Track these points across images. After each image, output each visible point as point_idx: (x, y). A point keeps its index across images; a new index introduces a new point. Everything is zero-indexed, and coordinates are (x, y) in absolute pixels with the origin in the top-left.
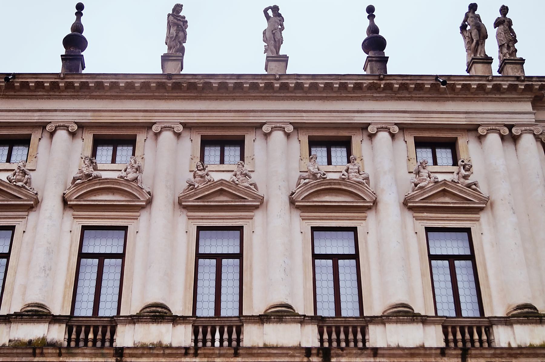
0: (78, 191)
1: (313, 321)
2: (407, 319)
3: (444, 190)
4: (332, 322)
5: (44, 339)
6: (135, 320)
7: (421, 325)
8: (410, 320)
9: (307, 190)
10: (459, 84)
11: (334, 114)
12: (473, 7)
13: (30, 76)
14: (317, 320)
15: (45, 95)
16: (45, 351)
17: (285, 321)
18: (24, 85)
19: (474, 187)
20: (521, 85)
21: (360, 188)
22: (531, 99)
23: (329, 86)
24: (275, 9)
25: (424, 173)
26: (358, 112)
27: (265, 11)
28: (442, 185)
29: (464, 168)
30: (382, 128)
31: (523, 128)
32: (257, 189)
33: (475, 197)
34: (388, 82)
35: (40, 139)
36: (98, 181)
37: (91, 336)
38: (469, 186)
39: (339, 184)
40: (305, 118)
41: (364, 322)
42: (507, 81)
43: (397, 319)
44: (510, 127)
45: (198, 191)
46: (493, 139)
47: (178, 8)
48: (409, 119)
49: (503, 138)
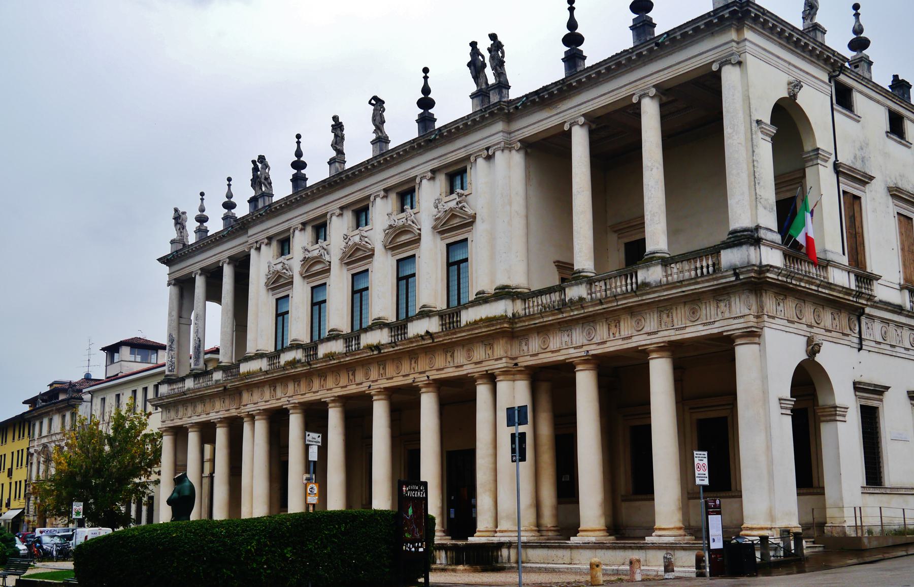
0: (304, 268)
5: (295, 358)
7: (427, 319)
9: (389, 237)
11: (402, 175)
12: (473, 45)
16: (296, 366)
23: (413, 148)
24: (375, 98)
25: (440, 206)
27: (370, 103)
28: (449, 213)
31: (494, 148)
33: (466, 215)
37: (312, 353)
38: (461, 208)
39: (403, 227)
42: (477, 115)
44: (487, 149)
47: (335, 118)
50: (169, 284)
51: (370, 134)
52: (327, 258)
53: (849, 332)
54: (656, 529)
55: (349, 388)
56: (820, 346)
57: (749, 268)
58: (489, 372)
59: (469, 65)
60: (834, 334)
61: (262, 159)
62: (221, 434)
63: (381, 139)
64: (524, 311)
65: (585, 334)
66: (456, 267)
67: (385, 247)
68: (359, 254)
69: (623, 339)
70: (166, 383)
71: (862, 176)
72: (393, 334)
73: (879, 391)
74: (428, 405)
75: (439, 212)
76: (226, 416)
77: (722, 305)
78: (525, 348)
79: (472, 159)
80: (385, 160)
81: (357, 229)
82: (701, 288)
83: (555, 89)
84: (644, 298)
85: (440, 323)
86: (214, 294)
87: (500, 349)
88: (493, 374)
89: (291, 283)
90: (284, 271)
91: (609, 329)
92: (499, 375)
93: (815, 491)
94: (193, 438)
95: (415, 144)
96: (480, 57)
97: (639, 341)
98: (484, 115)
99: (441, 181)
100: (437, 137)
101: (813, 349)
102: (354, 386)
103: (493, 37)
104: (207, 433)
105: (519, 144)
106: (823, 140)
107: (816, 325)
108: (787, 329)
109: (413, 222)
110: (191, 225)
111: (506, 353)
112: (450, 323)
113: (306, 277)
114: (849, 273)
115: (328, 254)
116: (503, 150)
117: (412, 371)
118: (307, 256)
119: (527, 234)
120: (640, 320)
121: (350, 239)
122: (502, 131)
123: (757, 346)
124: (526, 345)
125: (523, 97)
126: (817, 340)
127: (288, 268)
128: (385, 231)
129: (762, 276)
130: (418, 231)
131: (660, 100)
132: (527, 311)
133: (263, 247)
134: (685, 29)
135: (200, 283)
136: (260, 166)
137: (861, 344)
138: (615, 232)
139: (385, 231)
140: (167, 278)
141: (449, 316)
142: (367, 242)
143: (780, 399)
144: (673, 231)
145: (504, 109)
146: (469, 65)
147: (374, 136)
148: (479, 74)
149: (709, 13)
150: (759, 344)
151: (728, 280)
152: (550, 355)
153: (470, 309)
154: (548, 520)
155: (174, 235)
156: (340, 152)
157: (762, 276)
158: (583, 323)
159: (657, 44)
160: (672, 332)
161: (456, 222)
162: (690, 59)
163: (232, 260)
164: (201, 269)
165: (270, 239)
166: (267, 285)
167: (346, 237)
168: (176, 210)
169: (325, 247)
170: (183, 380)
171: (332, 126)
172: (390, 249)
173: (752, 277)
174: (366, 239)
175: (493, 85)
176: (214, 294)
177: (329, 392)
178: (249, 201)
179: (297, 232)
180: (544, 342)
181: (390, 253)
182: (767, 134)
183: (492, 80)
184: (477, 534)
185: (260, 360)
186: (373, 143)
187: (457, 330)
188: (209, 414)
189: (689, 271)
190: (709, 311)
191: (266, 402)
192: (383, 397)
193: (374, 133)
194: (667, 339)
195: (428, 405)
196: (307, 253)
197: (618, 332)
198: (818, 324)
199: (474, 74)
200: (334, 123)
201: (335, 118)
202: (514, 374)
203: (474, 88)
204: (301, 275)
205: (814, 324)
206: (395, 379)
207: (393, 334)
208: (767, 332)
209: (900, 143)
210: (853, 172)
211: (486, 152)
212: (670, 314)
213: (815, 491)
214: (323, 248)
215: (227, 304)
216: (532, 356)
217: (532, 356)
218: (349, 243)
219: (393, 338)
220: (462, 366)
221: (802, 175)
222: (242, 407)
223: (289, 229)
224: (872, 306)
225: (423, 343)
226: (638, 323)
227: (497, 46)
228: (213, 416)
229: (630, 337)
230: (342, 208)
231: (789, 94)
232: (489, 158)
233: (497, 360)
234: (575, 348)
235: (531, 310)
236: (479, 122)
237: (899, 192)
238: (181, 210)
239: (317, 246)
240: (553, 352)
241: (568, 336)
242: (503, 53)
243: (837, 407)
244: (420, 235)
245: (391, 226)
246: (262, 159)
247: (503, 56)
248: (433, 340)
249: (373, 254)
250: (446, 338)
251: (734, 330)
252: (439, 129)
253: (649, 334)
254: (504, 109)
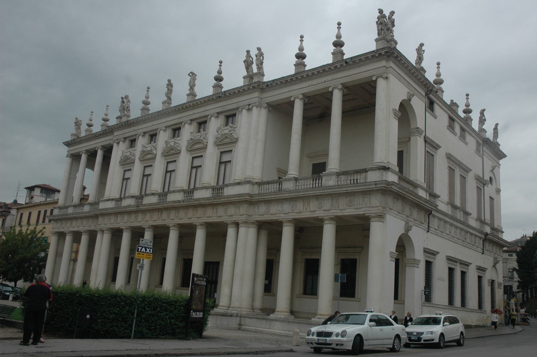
3: (226, 137)
12: (248, 52)
24: (191, 73)
25: (220, 132)
27: (189, 75)
38: (231, 134)
44: (249, 105)
47: (169, 81)
50: (67, 157)
51: (186, 90)
52: (155, 152)
53: (423, 221)
54: (318, 314)
55: (157, 221)
56: (412, 227)
57: (382, 182)
58: (236, 221)
59: (244, 62)
60: (417, 222)
61: (127, 97)
62: (84, 239)
63: (192, 94)
64: (258, 191)
65: (290, 207)
66: (224, 164)
67: (187, 149)
68: (173, 152)
69: (311, 212)
71: (436, 145)
72: (185, 195)
73: (434, 254)
74: (200, 236)
75: (219, 134)
76: (89, 229)
77: (366, 199)
78: (257, 211)
79: (240, 109)
80: (193, 104)
81: (173, 138)
82: (356, 189)
83: (289, 79)
84: (325, 191)
85: (212, 192)
86: (90, 164)
87: (244, 209)
88: (237, 223)
89: (134, 162)
90: (131, 156)
91: (304, 206)
92: (241, 223)
93: (399, 302)
94: (68, 239)
96: (251, 58)
97: (319, 214)
98: (249, 88)
99: (222, 120)
100: (223, 96)
101: (408, 229)
103: (259, 49)
104: (77, 237)
105: (266, 105)
106: (420, 124)
107: (410, 216)
108: (397, 216)
109: (204, 138)
110: (84, 127)
111: (246, 212)
112: (217, 193)
113: (142, 160)
114: (426, 192)
115: (155, 150)
116: (257, 107)
117: (194, 216)
118: (144, 150)
119: (264, 152)
120: (321, 203)
121: (168, 143)
122: (258, 97)
123: (382, 223)
124: (257, 209)
125: (271, 81)
126: (411, 224)
127: (133, 154)
128: (188, 141)
129: (389, 187)
130: (206, 143)
131: (343, 92)
132: (260, 191)
133: (121, 143)
134: (360, 57)
135: (84, 158)
136: (125, 100)
137: (429, 229)
138: (308, 157)
139: (188, 141)
140: (66, 153)
141: (218, 189)
142: (177, 146)
143: (391, 252)
144: (342, 160)
145: (260, 85)
146: (244, 62)
147: (188, 92)
148: (249, 66)
149: (374, 51)
150: (383, 222)
151: (370, 187)
152: (270, 216)
153: (229, 187)
154: (258, 304)
155: (74, 132)
156: (169, 98)
157: (389, 187)
158: (290, 201)
159: (346, 62)
160: (338, 211)
161: (227, 140)
162: (361, 72)
163: (103, 147)
164: (86, 150)
165: (125, 138)
166: (120, 162)
167: (167, 142)
168: (76, 119)
169: (154, 146)
170: (67, 207)
171: (167, 84)
172: (189, 151)
173: (384, 187)
174: (177, 144)
175: (256, 73)
176: (90, 164)
177: (147, 222)
178: (117, 118)
179: (140, 137)
180: (268, 209)
181: (189, 153)
182: (396, 116)
183: (255, 70)
184: (219, 307)
186: (188, 95)
187: (221, 197)
188: (79, 227)
189: (347, 180)
190: (359, 201)
191: (111, 224)
192: (176, 228)
193: (189, 90)
194: (335, 214)
195: (200, 236)
196: (144, 148)
197: (308, 208)
198: (411, 216)
199: (247, 66)
200: (168, 83)
201: (169, 81)
202: (249, 224)
203: (245, 73)
204: (140, 159)
205: (409, 216)
206: (184, 220)
207: (185, 195)
208: (388, 217)
209: (452, 132)
210: (432, 142)
211: (248, 106)
212: (338, 202)
213: (399, 302)
214: (153, 147)
216: (260, 215)
217: (260, 215)
218: (168, 145)
219: (185, 198)
220: (221, 217)
221: (408, 140)
222: (98, 225)
223: (136, 135)
224: (435, 211)
226: (320, 204)
227: (260, 54)
228: (81, 229)
229: (314, 211)
230: (166, 127)
231: (408, 98)
232: (249, 110)
233: (241, 215)
234: (284, 214)
235: (262, 191)
236: (246, 91)
237: (450, 156)
238: (79, 119)
239: (150, 145)
240: (272, 214)
241: (281, 207)
242: (263, 58)
243: (415, 260)
244: (207, 145)
245: (192, 139)
246: (127, 97)
247: (263, 59)
249: (180, 153)
250: (214, 200)
251: (371, 213)
252: (225, 92)
253: (325, 211)
254: (260, 85)
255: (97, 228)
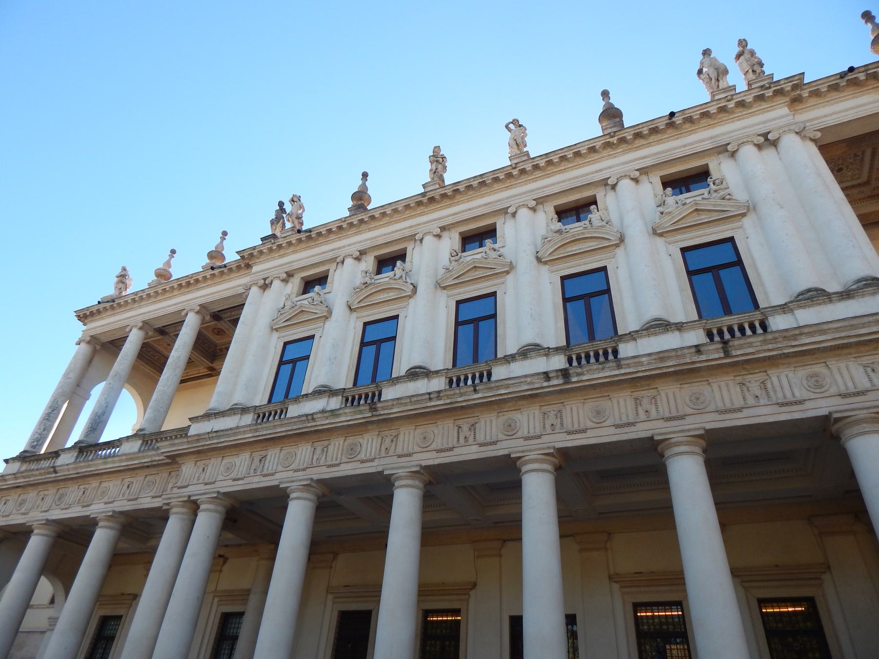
1: (559, 351)
2: (659, 330)
4: (579, 349)
6: (395, 382)
7: (677, 333)
8: (663, 330)
10: (696, 115)
13: (322, 227)
14: (563, 350)
15: (336, 238)
17: (530, 357)
18: (319, 234)
19: (728, 197)
20: (768, 93)
21: (603, 231)
22: (787, 103)
24: (515, 122)
26: (597, 172)
27: (507, 127)
29: (714, 184)
30: (622, 177)
32: (504, 258)
33: (732, 206)
34: (620, 137)
35: (335, 270)
36: (373, 286)
40: (546, 192)
41: (613, 342)
43: (648, 332)
45: (453, 273)
46: (748, 152)
47: (437, 149)
48: (650, 162)
49: (759, 147)
50: (78, 343)
55: (457, 451)
67: (539, 260)
70: (19, 461)
95: (616, 138)
102: (475, 448)
133: (277, 284)
164: (144, 322)
168: (124, 269)
185: (239, 416)
206: (590, 433)
215: (179, 357)
220: (801, 402)
225: (696, 359)
228: (97, 509)
230: (443, 229)
248: (727, 354)
255: (176, 496)
